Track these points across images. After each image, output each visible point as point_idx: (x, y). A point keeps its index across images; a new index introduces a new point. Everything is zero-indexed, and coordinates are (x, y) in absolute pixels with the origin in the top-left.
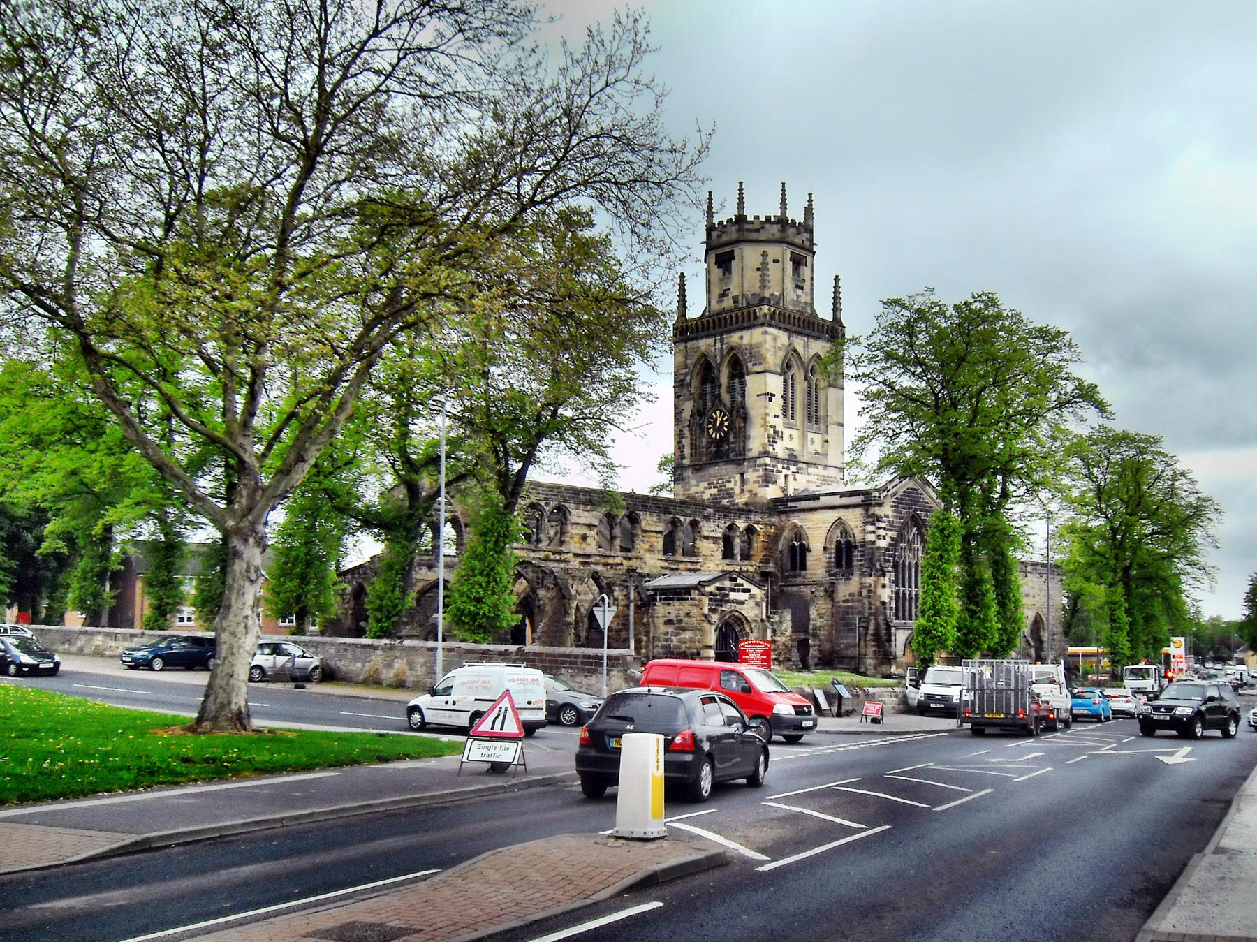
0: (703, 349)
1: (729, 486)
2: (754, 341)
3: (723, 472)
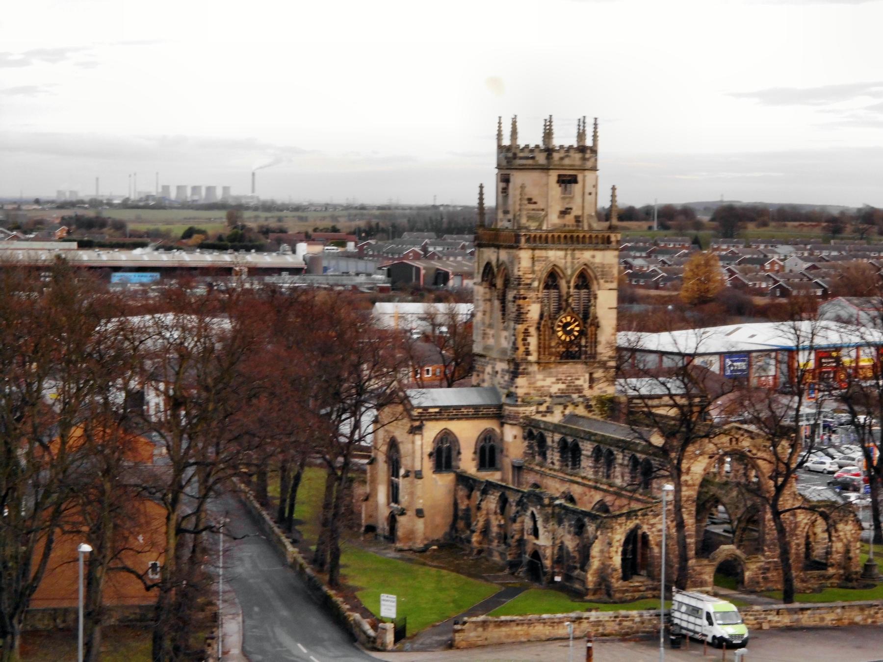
1: (578, 383)
2: (606, 262)
3: (573, 371)
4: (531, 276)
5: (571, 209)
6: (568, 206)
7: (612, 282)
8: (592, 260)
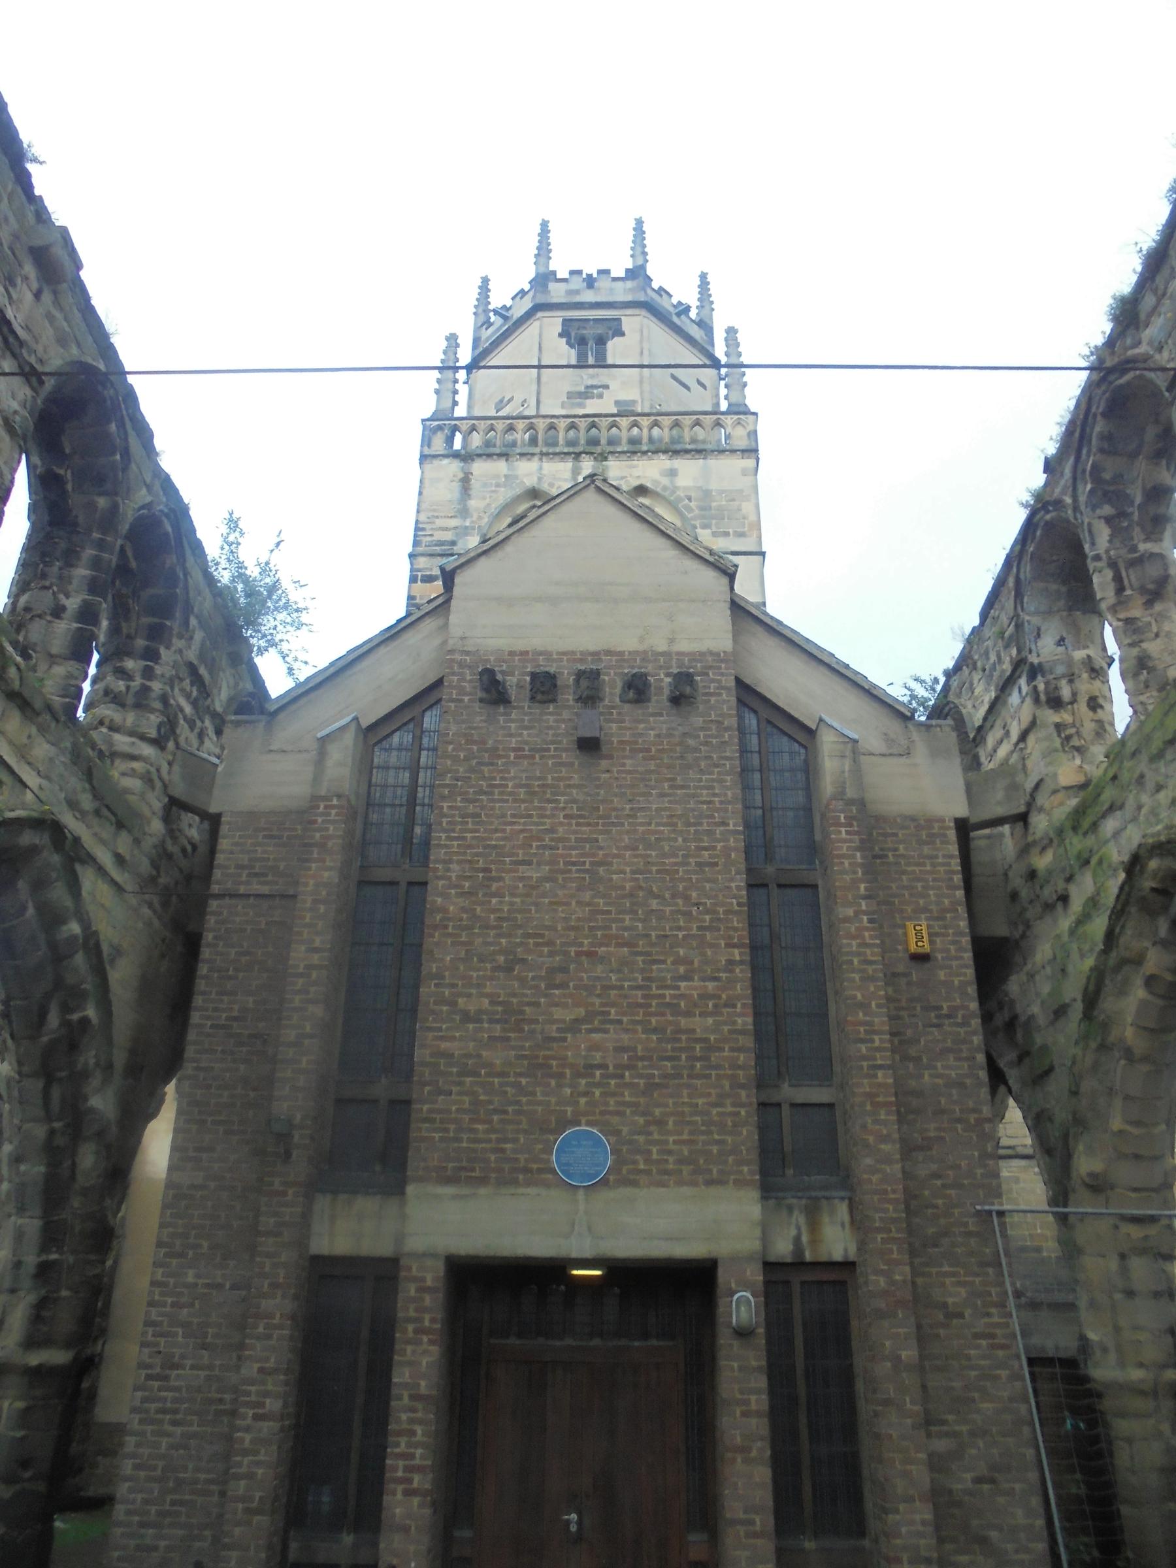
0: (530, 482)
4: (454, 523)
5: (607, 387)
6: (590, 382)
7: (742, 535)
8: (665, 481)
